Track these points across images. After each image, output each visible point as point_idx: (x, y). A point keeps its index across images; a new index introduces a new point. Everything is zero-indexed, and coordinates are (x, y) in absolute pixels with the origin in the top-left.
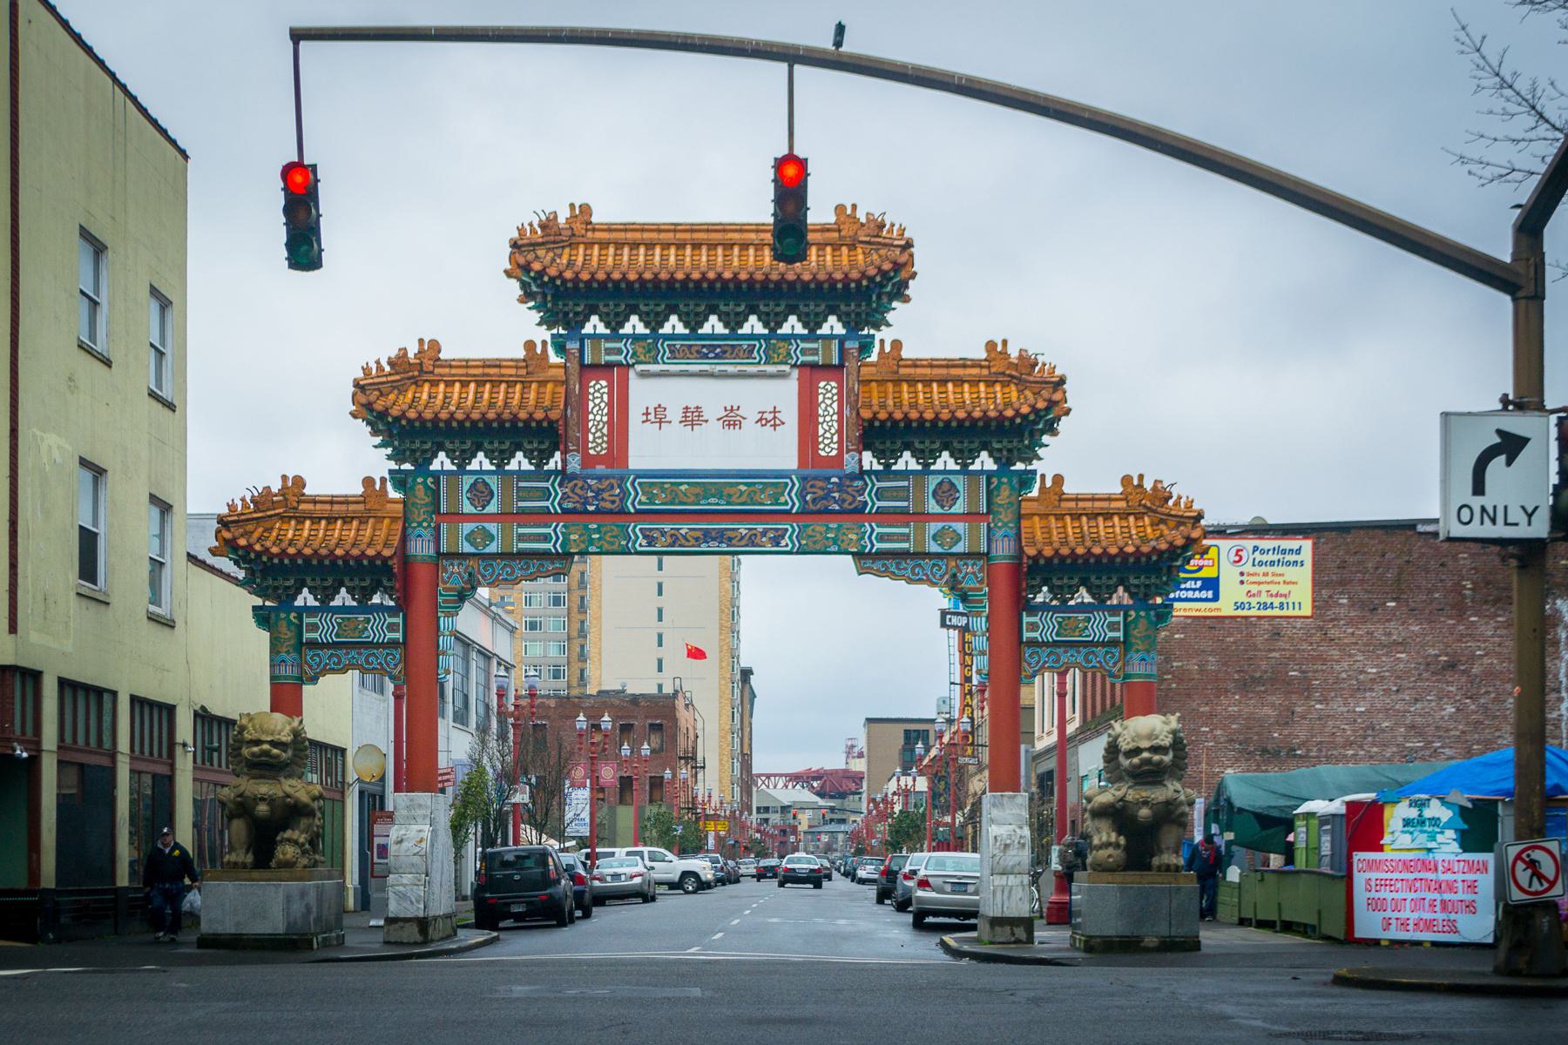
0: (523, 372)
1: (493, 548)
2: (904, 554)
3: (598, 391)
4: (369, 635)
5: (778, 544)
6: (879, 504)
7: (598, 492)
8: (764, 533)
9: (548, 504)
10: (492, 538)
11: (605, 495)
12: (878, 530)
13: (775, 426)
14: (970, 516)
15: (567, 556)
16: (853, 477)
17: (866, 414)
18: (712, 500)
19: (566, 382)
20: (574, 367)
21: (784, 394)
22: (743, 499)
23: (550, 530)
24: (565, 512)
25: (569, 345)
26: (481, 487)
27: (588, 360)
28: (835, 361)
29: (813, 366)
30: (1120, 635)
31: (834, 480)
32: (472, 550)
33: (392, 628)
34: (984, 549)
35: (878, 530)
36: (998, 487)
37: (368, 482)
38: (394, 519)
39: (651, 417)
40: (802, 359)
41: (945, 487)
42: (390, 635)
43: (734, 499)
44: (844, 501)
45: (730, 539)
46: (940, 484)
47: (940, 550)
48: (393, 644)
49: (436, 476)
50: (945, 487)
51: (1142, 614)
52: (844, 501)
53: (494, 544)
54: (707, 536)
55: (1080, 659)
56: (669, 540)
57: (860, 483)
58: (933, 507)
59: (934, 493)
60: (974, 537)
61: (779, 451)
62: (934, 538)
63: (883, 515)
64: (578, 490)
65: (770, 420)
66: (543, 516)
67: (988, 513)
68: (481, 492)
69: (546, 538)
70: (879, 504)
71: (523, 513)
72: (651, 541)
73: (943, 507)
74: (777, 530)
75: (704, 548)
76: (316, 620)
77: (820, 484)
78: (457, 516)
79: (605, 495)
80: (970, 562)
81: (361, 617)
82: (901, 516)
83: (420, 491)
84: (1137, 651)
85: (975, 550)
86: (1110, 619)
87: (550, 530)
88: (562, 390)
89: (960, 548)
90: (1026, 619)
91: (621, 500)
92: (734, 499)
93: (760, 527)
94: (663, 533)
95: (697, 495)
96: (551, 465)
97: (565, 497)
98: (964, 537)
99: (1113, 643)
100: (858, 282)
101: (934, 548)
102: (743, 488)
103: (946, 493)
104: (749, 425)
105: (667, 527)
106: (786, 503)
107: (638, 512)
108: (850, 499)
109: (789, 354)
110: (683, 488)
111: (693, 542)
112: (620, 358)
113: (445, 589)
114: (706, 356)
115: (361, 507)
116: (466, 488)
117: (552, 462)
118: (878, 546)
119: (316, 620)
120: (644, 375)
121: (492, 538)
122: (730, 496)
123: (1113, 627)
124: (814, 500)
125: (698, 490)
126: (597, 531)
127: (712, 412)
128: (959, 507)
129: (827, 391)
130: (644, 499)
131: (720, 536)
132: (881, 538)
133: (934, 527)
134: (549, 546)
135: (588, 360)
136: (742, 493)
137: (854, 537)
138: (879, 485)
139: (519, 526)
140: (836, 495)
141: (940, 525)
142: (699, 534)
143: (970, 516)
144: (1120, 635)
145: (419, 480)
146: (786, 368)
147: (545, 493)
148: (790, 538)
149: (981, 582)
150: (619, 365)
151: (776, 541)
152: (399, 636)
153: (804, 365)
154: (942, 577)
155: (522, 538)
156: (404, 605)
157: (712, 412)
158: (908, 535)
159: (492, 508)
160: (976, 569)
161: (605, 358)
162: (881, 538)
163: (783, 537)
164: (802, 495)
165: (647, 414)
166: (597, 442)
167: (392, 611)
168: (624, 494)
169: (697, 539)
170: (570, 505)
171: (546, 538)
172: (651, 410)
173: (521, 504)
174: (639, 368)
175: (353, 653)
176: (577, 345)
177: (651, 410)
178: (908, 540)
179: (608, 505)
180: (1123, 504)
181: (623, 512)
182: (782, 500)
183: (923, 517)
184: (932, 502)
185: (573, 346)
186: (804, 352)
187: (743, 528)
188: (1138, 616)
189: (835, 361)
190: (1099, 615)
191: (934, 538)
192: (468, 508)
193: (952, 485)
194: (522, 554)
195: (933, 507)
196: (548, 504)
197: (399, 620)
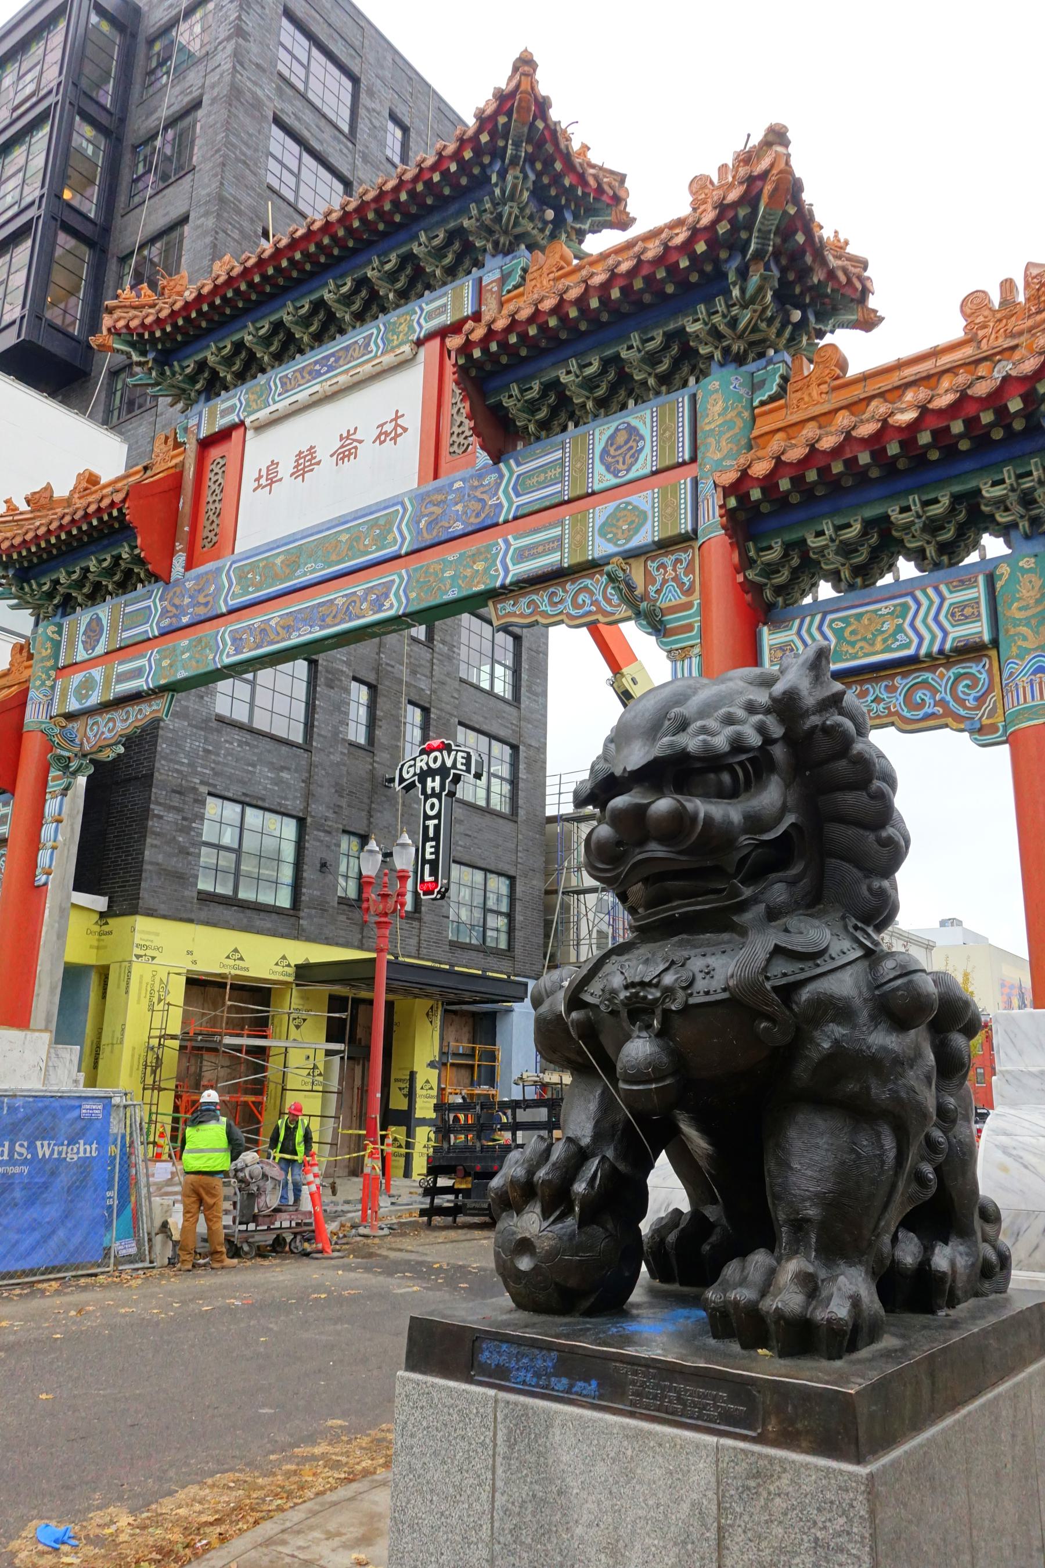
5: (379, 611)
13: (394, 439)
31: (456, 486)
35: (516, 544)
39: (263, 481)
41: (621, 439)
50: (621, 439)
55: (897, 701)
57: (494, 476)
59: (605, 452)
60: (667, 508)
62: (603, 534)
67: (694, 459)
70: (519, 501)
73: (616, 476)
80: (669, 560)
85: (670, 532)
86: (952, 598)
90: (769, 638)
93: (359, 589)
99: (970, 651)
100: (457, 156)
112: (233, 418)
120: (261, 428)
123: (962, 613)
124: (429, 524)
128: (643, 465)
132: (521, 555)
141: (611, 506)
149: (689, 592)
150: (235, 427)
157: (326, 448)
160: (681, 568)
162: (521, 555)
165: (258, 480)
173: (125, 635)
177: (264, 473)
180: (968, 351)
184: (599, 468)
193: (632, 430)
195: (601, 478)
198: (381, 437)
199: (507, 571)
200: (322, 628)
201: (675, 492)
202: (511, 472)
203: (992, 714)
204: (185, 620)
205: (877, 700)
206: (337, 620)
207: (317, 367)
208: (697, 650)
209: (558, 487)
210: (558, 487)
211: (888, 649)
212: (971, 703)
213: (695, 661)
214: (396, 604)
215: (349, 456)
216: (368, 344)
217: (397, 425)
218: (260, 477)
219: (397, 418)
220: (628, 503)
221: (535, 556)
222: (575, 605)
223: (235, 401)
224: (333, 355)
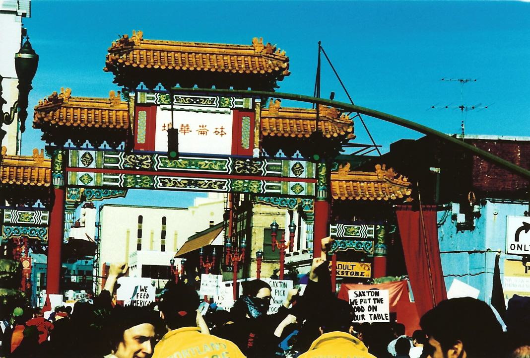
0: (109, 105)
1: (92, 184)
2: (278, 195)
3: (143, 115)
4: (33, 221)
5: (222, 189)
6: (267, 172)
7: (141, 161)
8: (215, 183)
9: (118, 165)
10: (92, 179)
11: (144, 162)
12: (266, 184)
13: (222, 135)
14: (308, 180)
15: (125, 189)
16: (256, 159)
17: (265, 134)
18: (193, 167)
19: (128, 111)
20: (132, 104)
21: (226, 121)
22: (207, 167)
23: (118, 177)
24: (126, 169)
25: (130, 94)
26: (88, 157)
27: (139, 101)
28: (250, 107)
29: (240, 109)
30: (373, 236)
31: (248, 160)
32: (83, 184)
33: (43, 218)
34: (314, 194)
35: (266, 184)
36: (321, 168)
37: (36, 151)
38: (47, 168)
40: (235, 106)
41: (298, 166)
42: (43, 221)
43: (202, 167)
44: (252, 170)
45: (200, 185)
46: (295, 165)
47: (294, 194)
48: (44, 225)
49: (67, 150)
50: (298, 166)
51: (383, 227)
52: (252, 170)
53: (93, 182)
54: (190, 183)
56: (173, 184)
57: (259, 163)
58: (292, 175)
59: (293, 169)
61: (224, 146)
62: (292, 189)
63: (270, 178)
64: (132, 160)
65: (221, 132)
66: (115, 171)
68: (88, 159)
69: (117, 180)
70: (267, 172)
71: (106, 168)
72: (164, 184)
73: (296, 175)
74: (221, 182)
75: (188, 188)
76: (10, 213)
77: (241, 162)
78: (76, 169)
79: (144, 162)
81: (30, 213)
82: (278, 178)
83: (60, 157)
84: (380, 243)
86: (368, 229)
87: (118, 177)
88: (126, 114)
89: (303, 194)
91: (151, 165)
92: (202, 167)
93: (214, 180)
94: (170, 181)
95: (186, 164)
96: (119, 148)
97: (126, 162)
98: (307, 189)
99: (370, 239)
101: (292, 193)
102: (207, 162)
103: (297, 170)
104: (211, 133)
105: (172, 178)
106: (226, 170)
107: (159, 170)
108: (255, 170)
109: (230, 103)
110: (180, 161)
111: (183, 185)
112: (154, 101)
113: (68, 201)
114: (192, 103)
115: (32, 162)
116: (81, 156)
117: (120, 146)
118: (266, 191)
119: (10, 213)
121: (92, 179)
122: (201, 165)
125: (186, 162)
126: (139, 178)
127: (194, 127)
129: (246, 121)
130: (162, 165)
131: (196, 184)
132: (268, 187)
133: (292, 184)
134: (118, 184)
135: (139, 101)
136: (206, 164)
137: (256, 187)
138: (268, 163)
139: (104, 174)
140: (249, 167)
141: (294, 183)
142: (186, 182)
143: (308, 180)
144: (373, 236)
145: (60, 152)
146: (229, 110)
147: (117, 161)
148: (227, 185)
149: (311, 209)
151: (220, 187)
152: (47, 222)
153: (236, 108)
154: (294, 206)
155: (105, 180)
156: (49, 208)
158: (280, 187)
159: (92, 166)
161: (147, 101)
162: (268, 187)
163: (224, 185)
164: (233, 166)
165: (164, 127)
166: (141, 138)
167: (44, 210)
168: (153, 162)
169: (185, 184)
170: (128, 166)
171: (117, 180)
172: (166, 125)
174: (162, 106)
175: (25, 228)
176: (134, 95)
177: (166, 125)
178: (280, 189)
179: (145, 167)
181: (152, 169)
182: (224, 168)
183: (288, 179)
184: (291, 172)
185: (132, 95)
186: (236, 103)
187: (206, 180)
188: (381, 228)
189: (250, 107)
190: (364, 226)
191: (292, 189)
192: (81, 165)
193: (301, 165)
194: (105, 187)
195: (292, 175)
196: (118, 165)
197: (47, 215)
198: (216, 132)
199: (264, 191)
200: (199, 188)
201: (312, 186)
202: (265, 163)
203: (372, 252)
204: (138, 168)
205: (351, 244)
206: (205, 187)
207: (192, 100)
208: (313, 223)
209: (280, 173)
210: (280, 173)
211: (355, 235)
212: (368, 249)
213: (312, 226)
214: (227, 189)
215: (204, 133)
216: (213, 102)
217: (222, 131)
218: (164, 127)
219: (222, 129)
220: (299, 184)
221: (271, 189)
222: (282, 204)
223: (154, 96)
224: (199, 98)
